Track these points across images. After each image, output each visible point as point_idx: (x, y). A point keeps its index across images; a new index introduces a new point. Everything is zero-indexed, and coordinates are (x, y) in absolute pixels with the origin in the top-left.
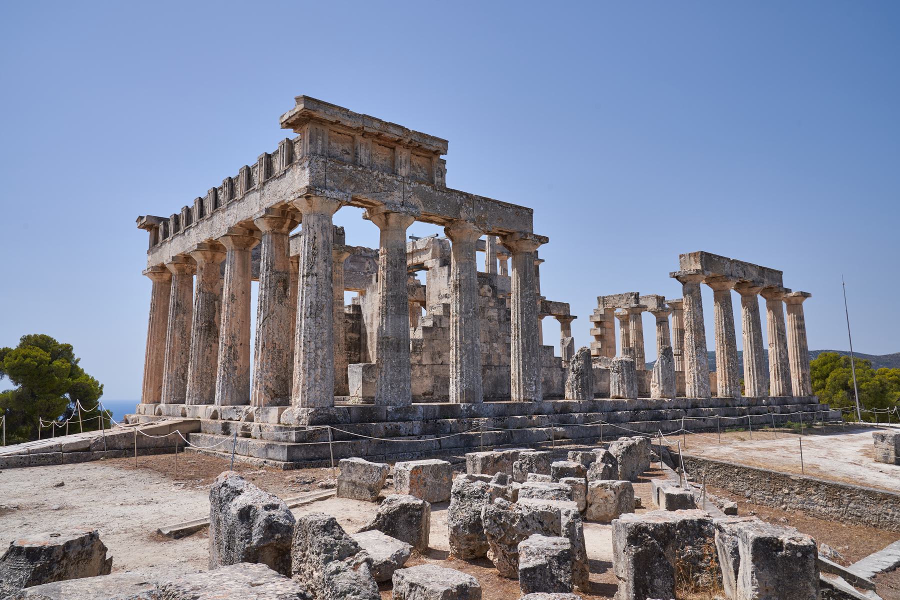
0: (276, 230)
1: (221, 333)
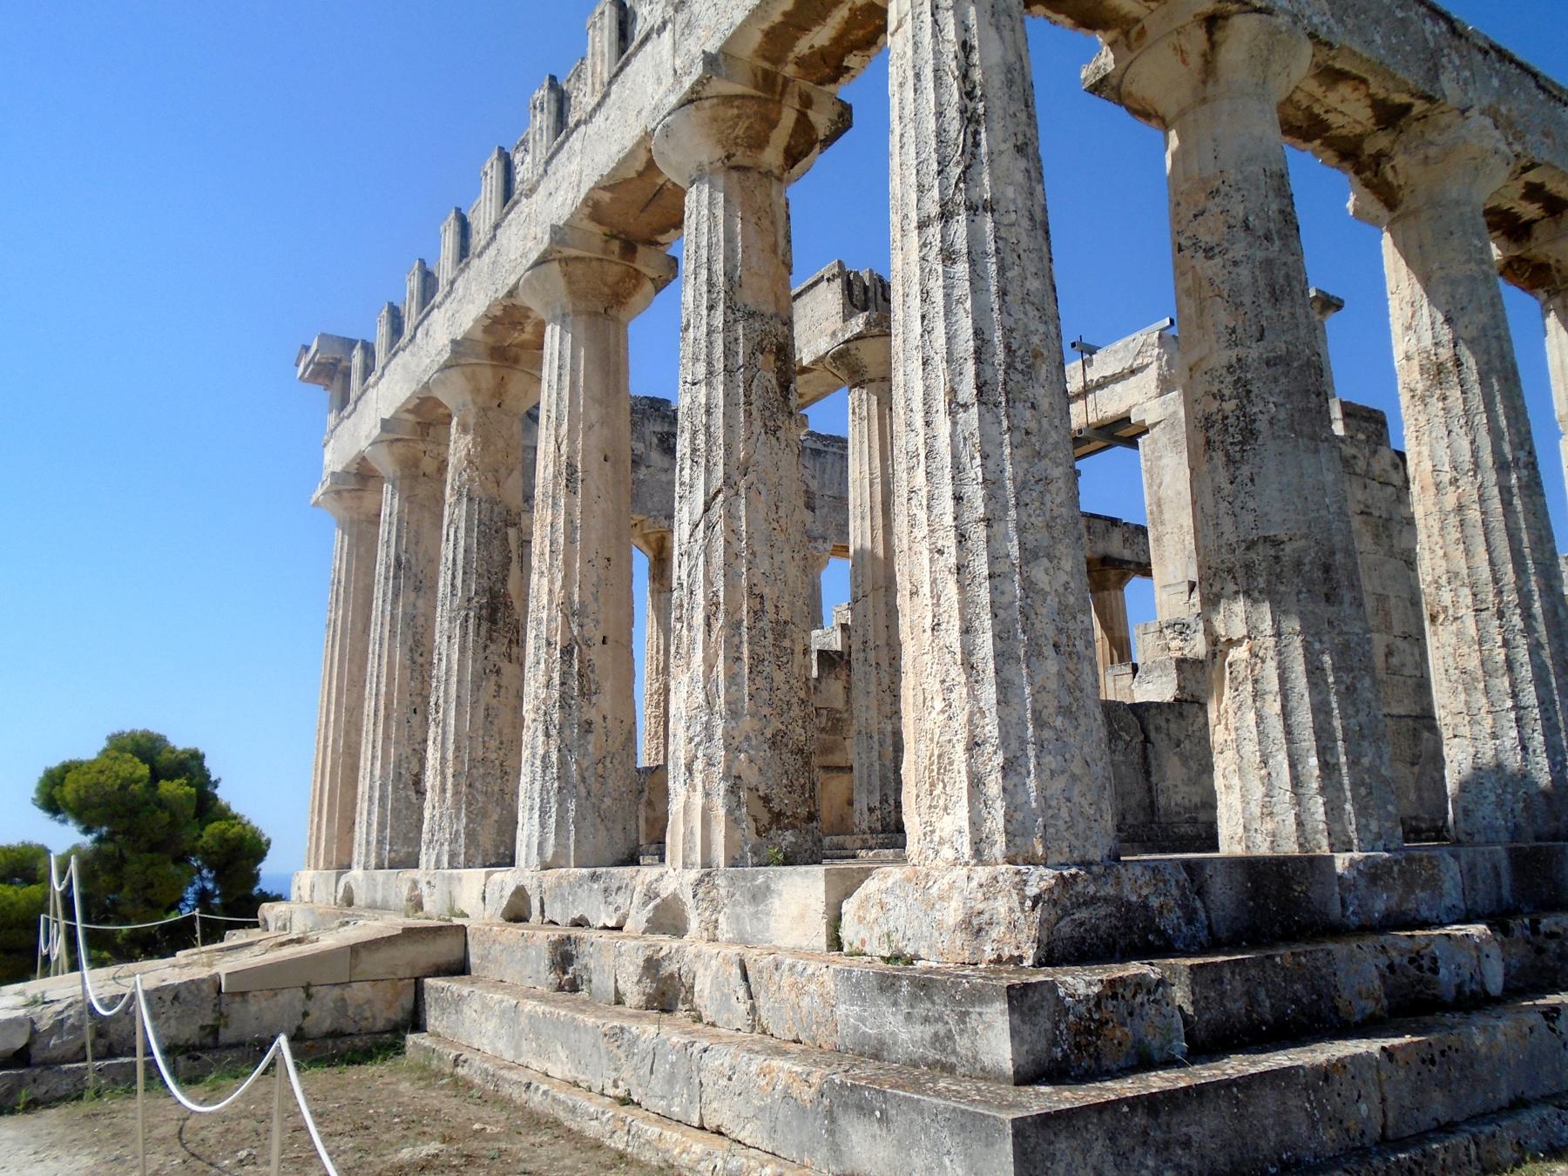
0: (739, 159)
1: (532, 605)
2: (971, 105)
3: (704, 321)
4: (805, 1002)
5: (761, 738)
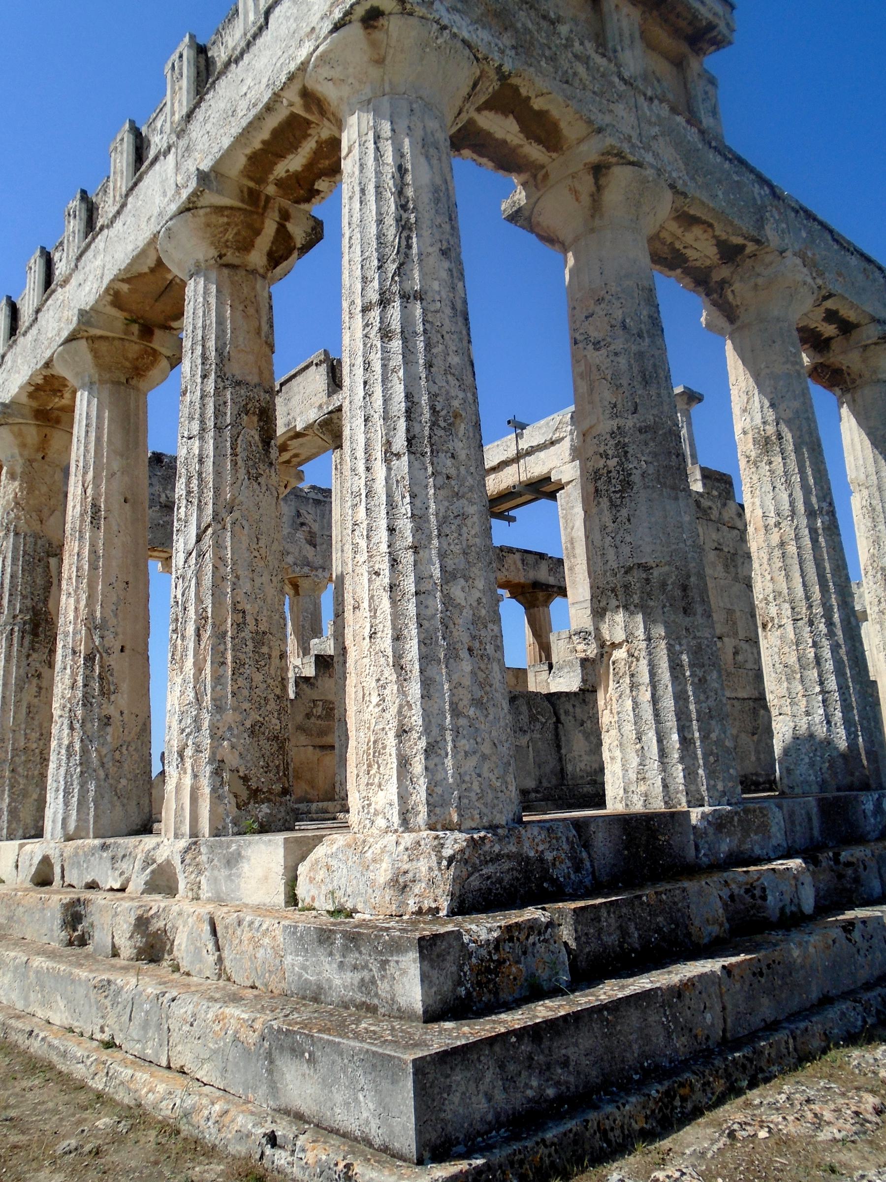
0: (231, 257)
1: (61, 621)
2: (405, 216)
3: (198, 388)
4: (261, 953)
5: (242, 728)
